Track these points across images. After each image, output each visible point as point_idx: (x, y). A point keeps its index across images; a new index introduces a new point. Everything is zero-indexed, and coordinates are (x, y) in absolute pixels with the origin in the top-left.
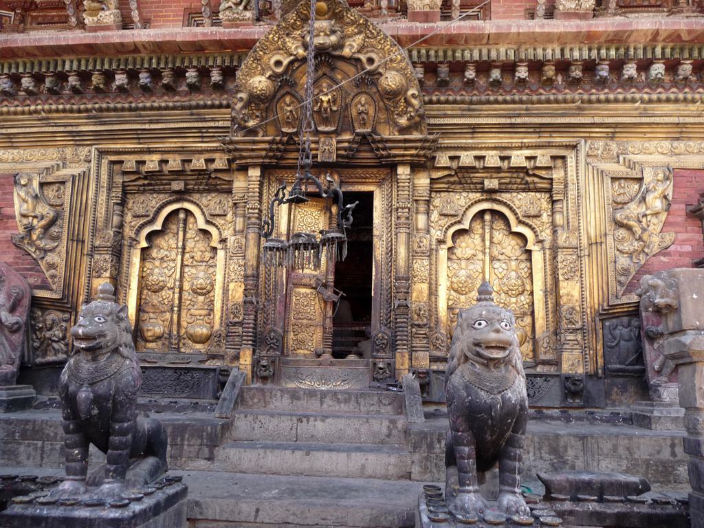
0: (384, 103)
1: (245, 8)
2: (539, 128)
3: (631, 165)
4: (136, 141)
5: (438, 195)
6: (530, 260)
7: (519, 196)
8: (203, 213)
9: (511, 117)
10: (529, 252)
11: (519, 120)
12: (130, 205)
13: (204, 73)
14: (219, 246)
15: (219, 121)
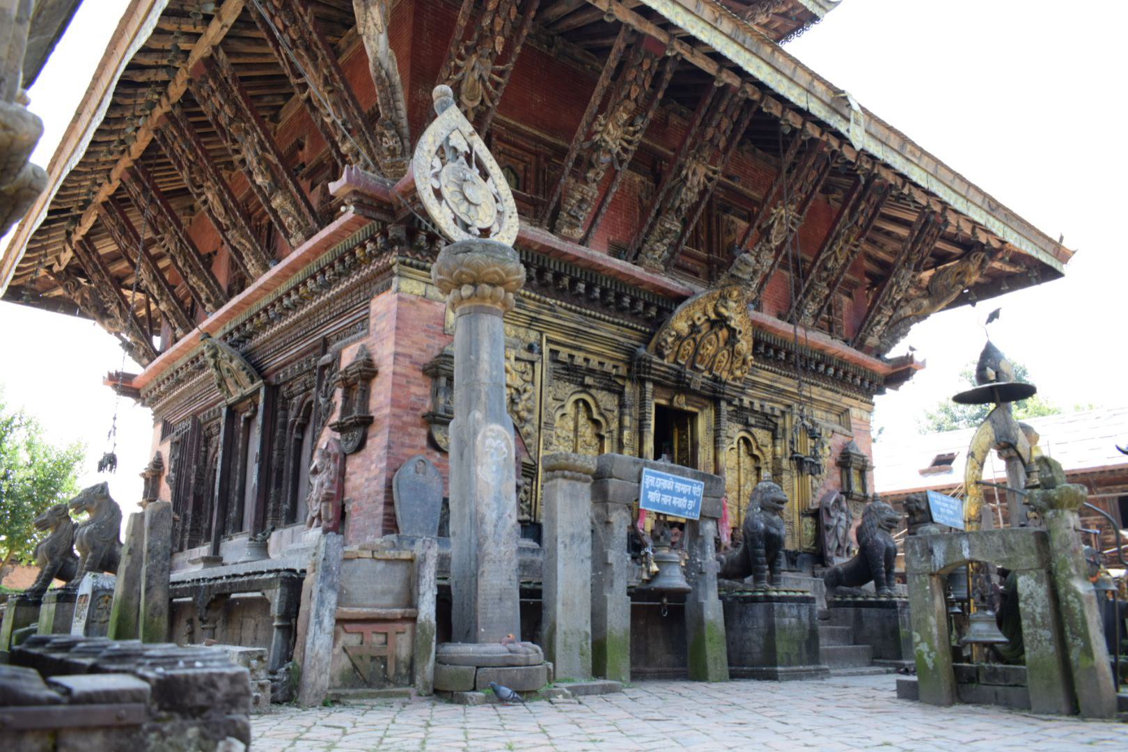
14: (607, 435)
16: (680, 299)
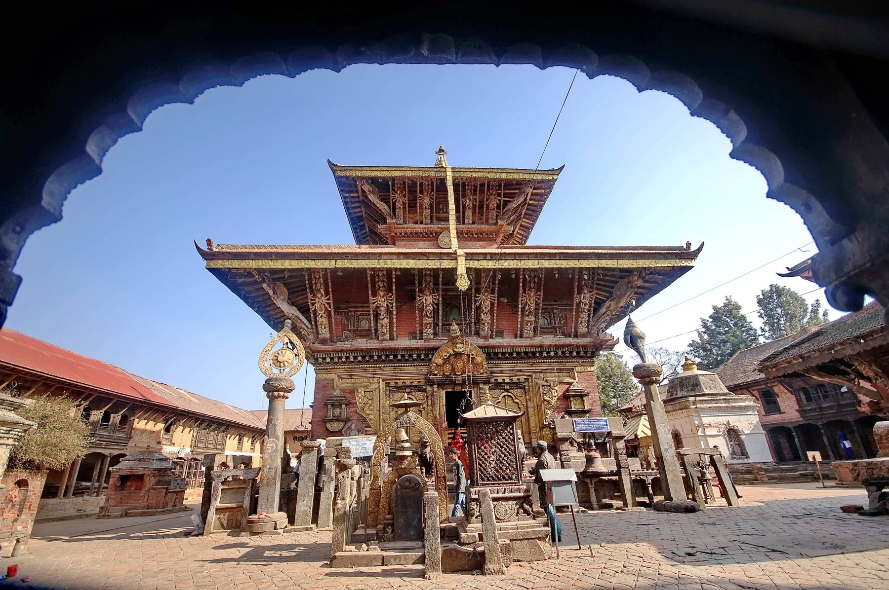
2: (520, 371)
3: (547, 381)
13: (419, 356)
16: (435, 349)
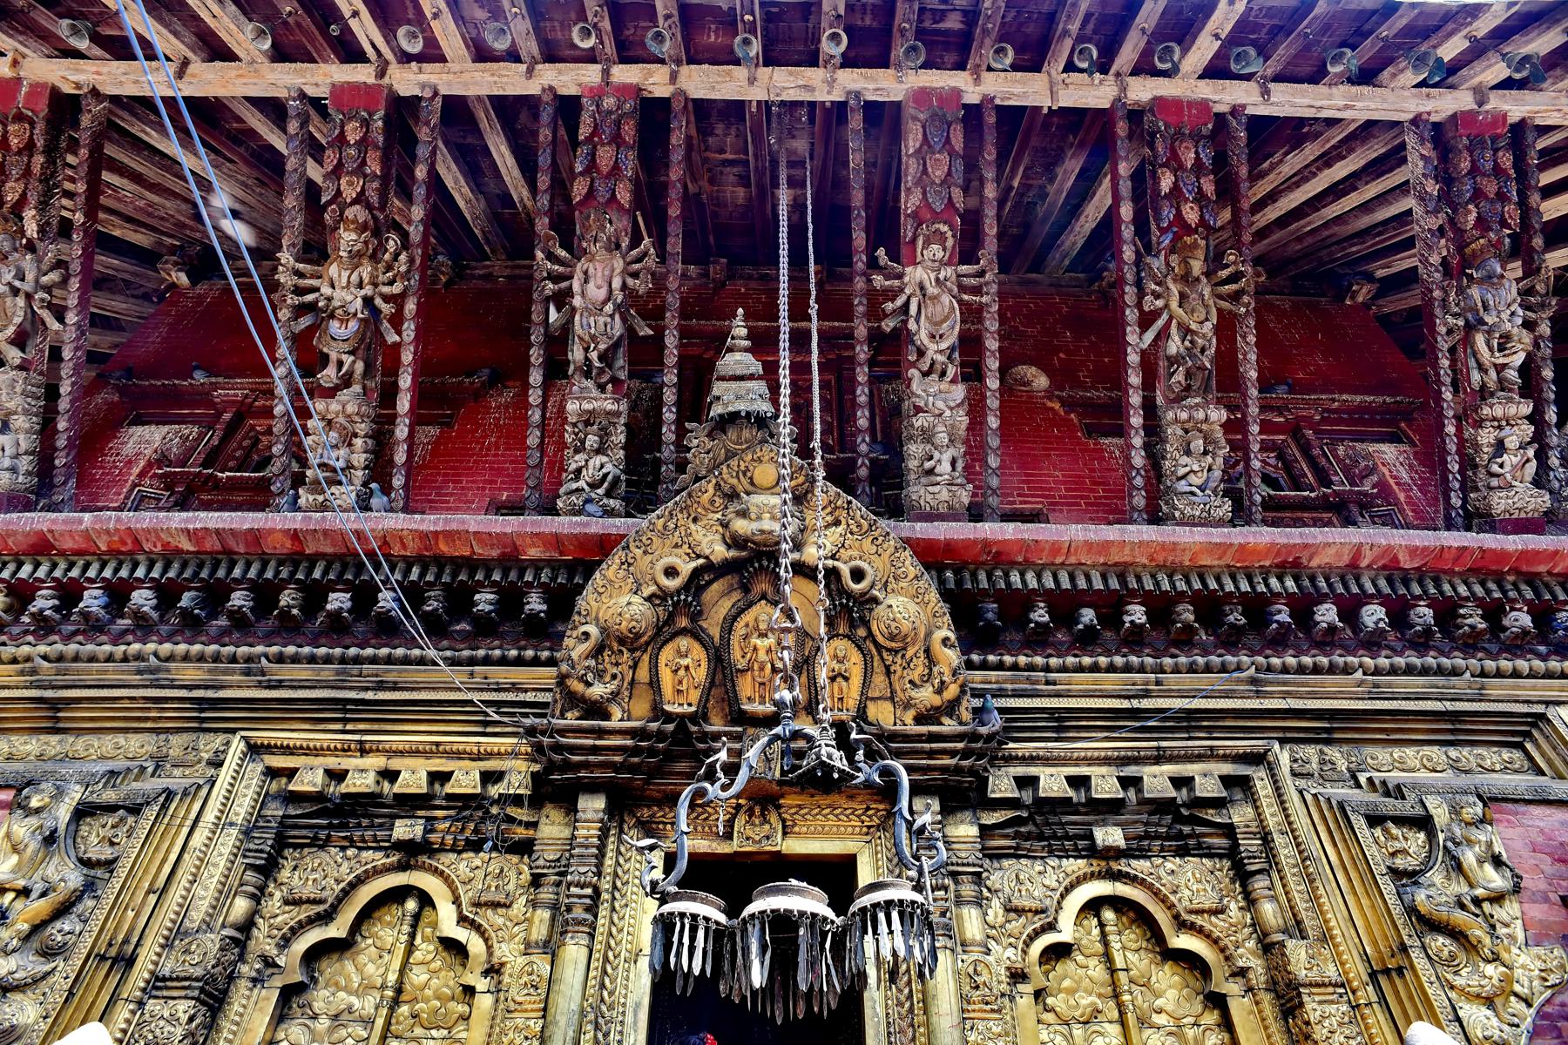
0: (883, 659)
1: (608, 494)
2: (1189, 721)
4: (339, 727)
5: (996, 865)
6: (1227, 1024)
7: (1169, 866)
8: (457, 901)
9: (1128, 697)
10: (1217, 1001)
11: (1146, 704)
12: (284, 875)
13: (511, 599)
14: (481, 984)
15: (526, 691)
